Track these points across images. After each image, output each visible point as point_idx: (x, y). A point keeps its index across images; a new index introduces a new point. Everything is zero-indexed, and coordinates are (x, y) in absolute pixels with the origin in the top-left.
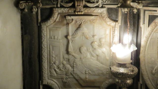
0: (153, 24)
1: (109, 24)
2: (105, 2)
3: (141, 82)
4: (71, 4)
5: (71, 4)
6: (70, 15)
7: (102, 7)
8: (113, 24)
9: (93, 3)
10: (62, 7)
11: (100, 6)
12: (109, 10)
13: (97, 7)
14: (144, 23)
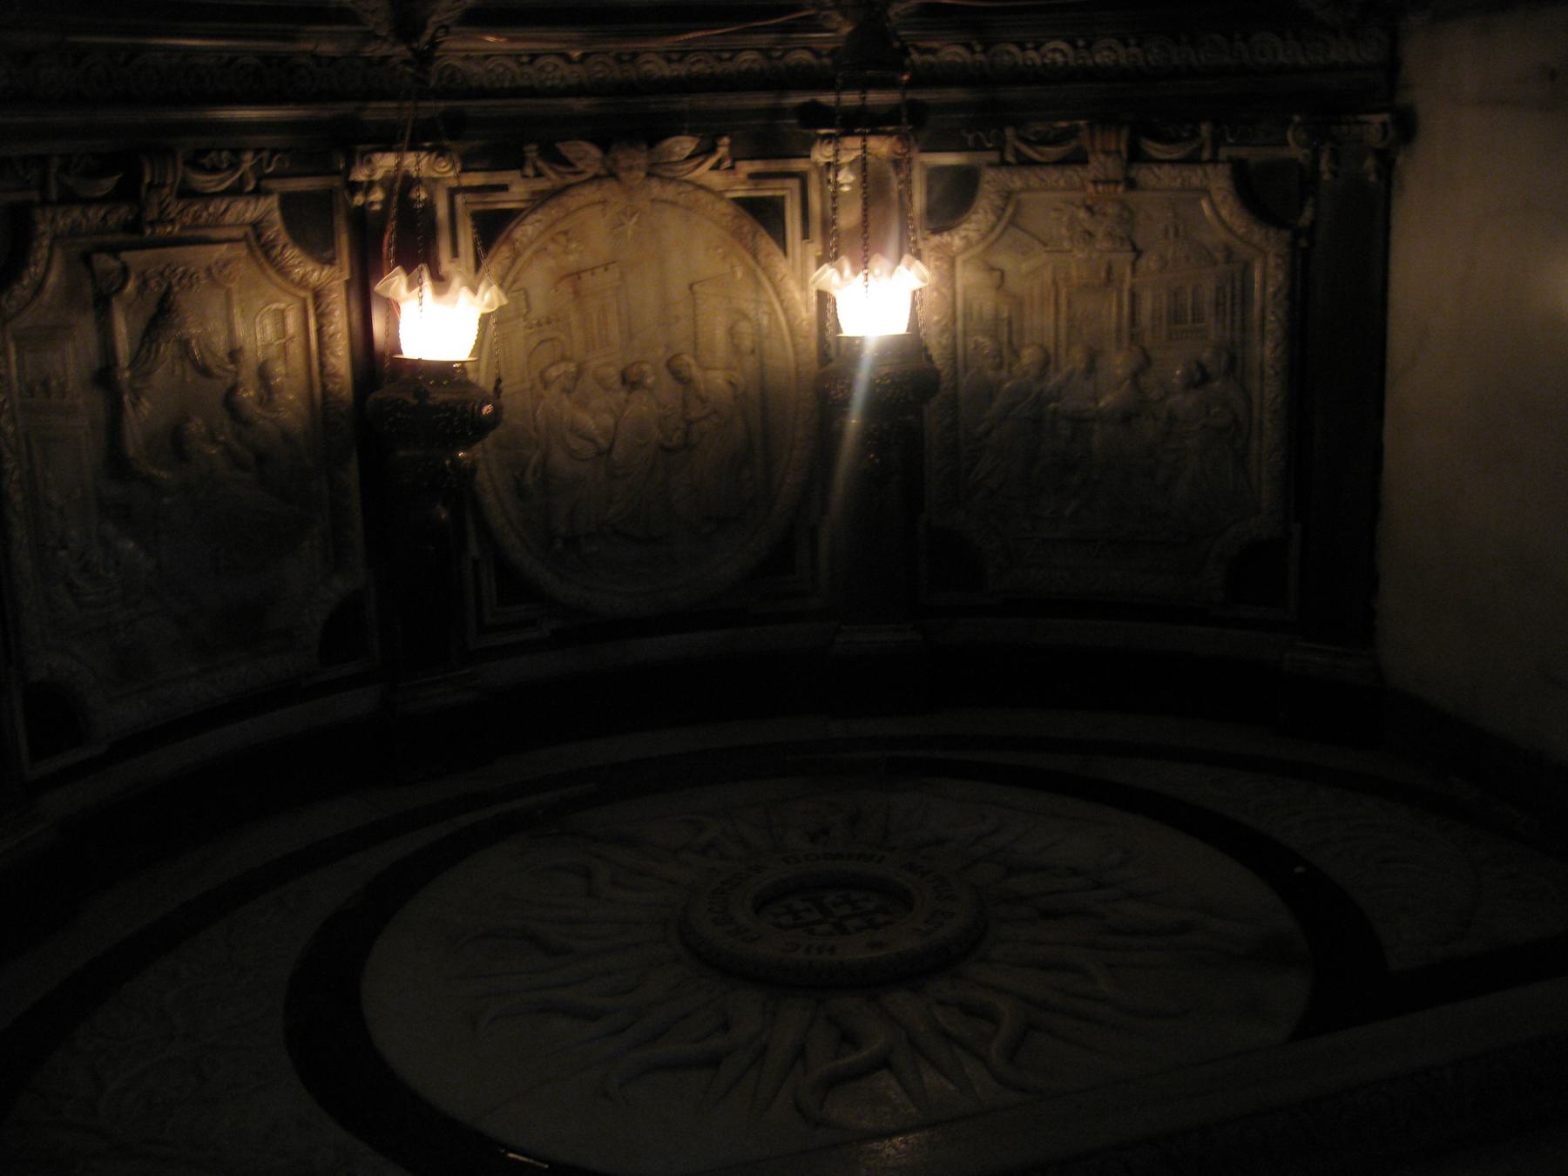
1: (297, 278)
2: (269, 165)
3: (474, 549)
4: (108, 184)
5: (108, 184)
6: (115, 250)
7: (259, 192)
9: (215, 170)
10: (69, 198)
12: (290, 204)
13: (236, 191)
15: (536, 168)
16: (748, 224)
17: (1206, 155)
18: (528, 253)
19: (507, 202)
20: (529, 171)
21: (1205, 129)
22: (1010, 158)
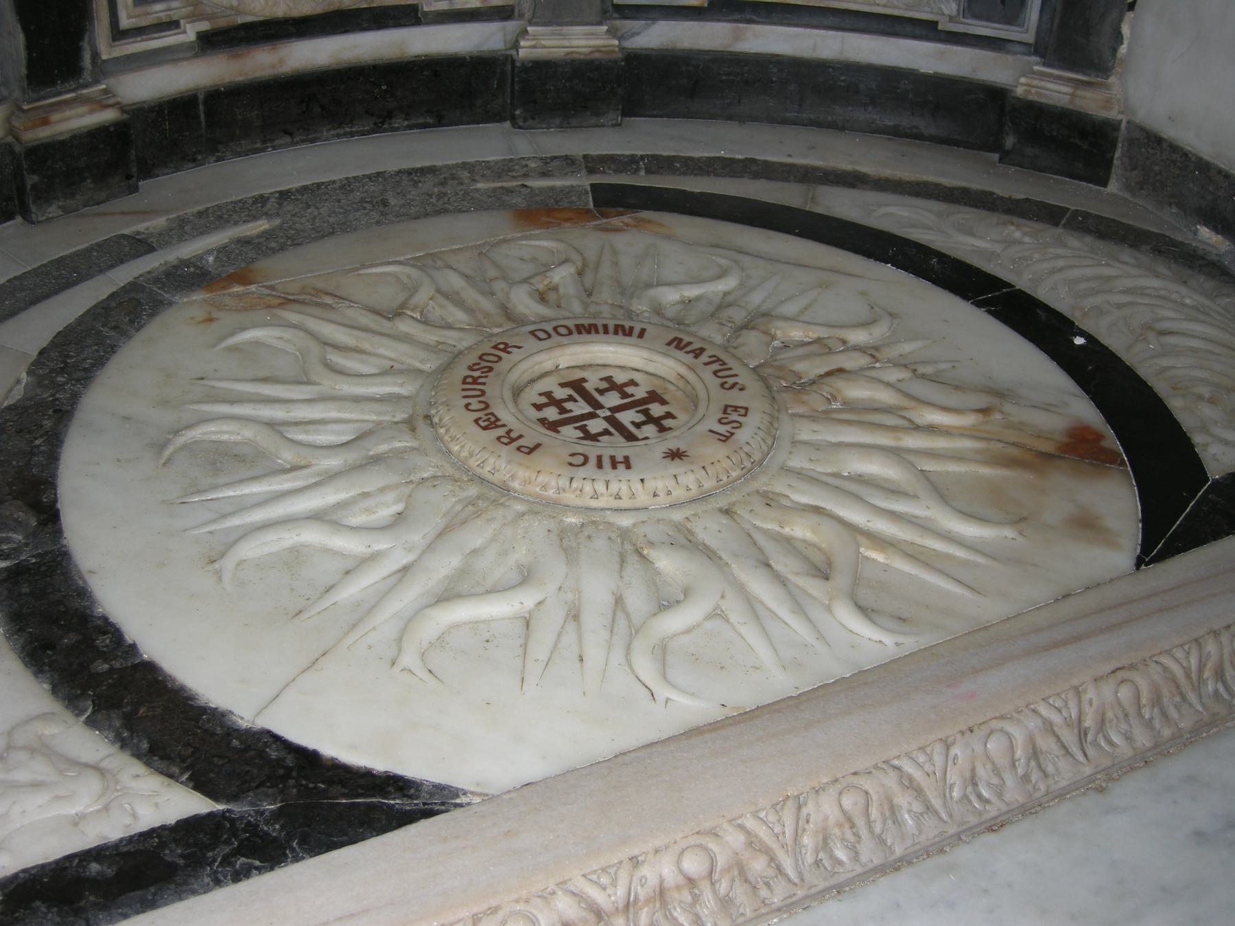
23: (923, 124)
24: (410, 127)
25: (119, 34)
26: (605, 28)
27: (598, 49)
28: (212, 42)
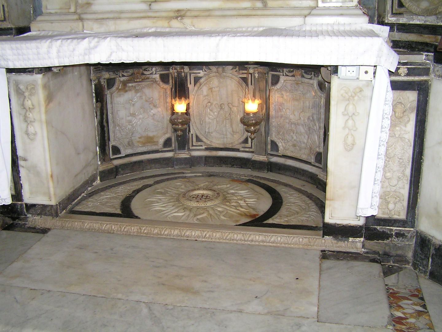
0: (198, 84)
1: (162, 87)
2: (158, 70)
7: (156, 74)
8: (165, 86)
11: (154, 73)
14: (191, 84)
15: (205, 70)
16: (241, 81)
17: (313, 78)
18: (203, 84)
19: (199, 75)
20: (204, 70)
21: (313, 73)
22: (284, 74)
23: (309, 180)
24: (237, 168)
25: (193, 146)
26: (265, 157)
27: (264, 160)
28: (207, 149)
